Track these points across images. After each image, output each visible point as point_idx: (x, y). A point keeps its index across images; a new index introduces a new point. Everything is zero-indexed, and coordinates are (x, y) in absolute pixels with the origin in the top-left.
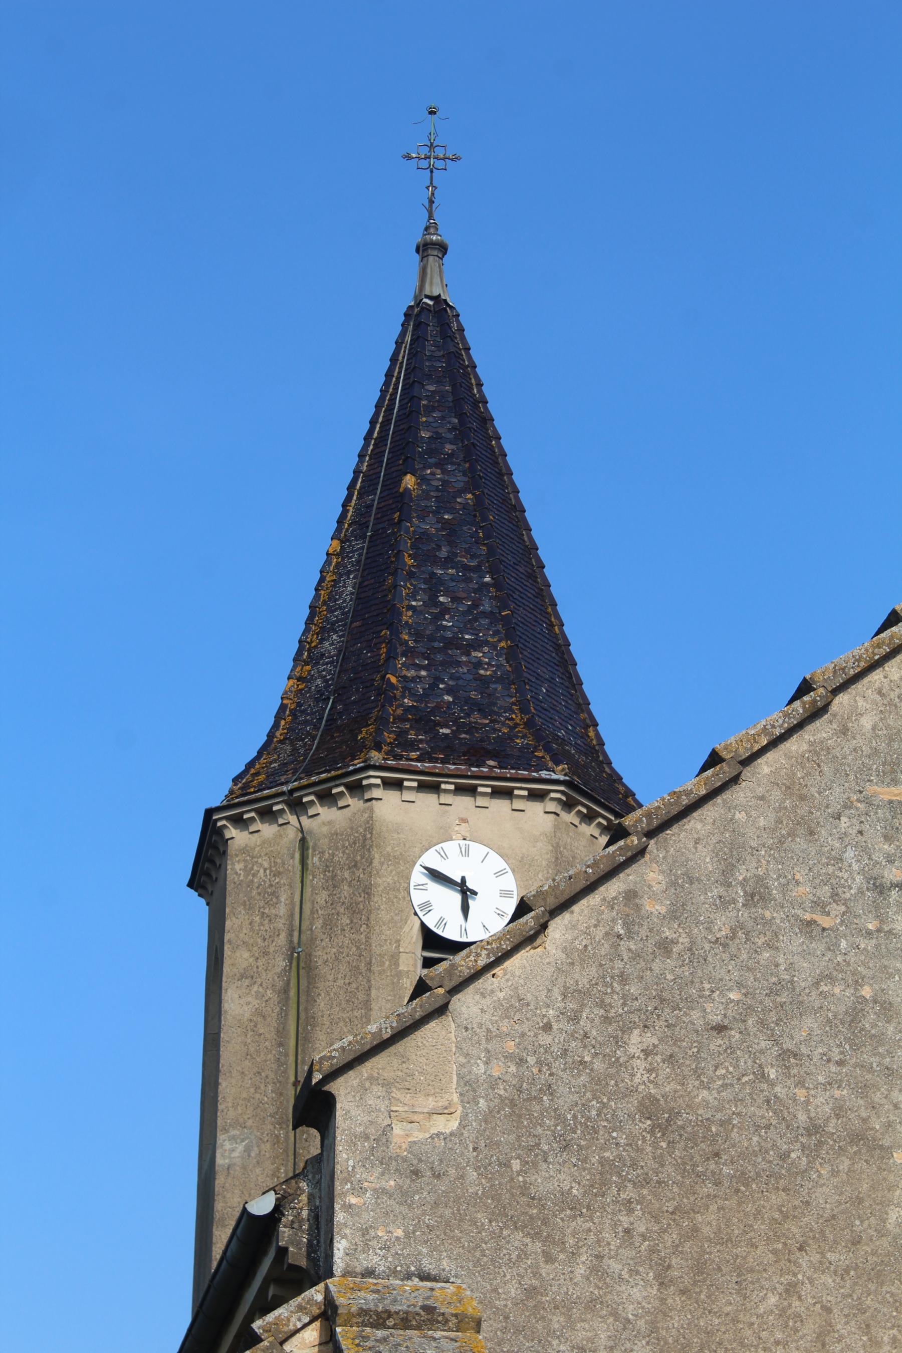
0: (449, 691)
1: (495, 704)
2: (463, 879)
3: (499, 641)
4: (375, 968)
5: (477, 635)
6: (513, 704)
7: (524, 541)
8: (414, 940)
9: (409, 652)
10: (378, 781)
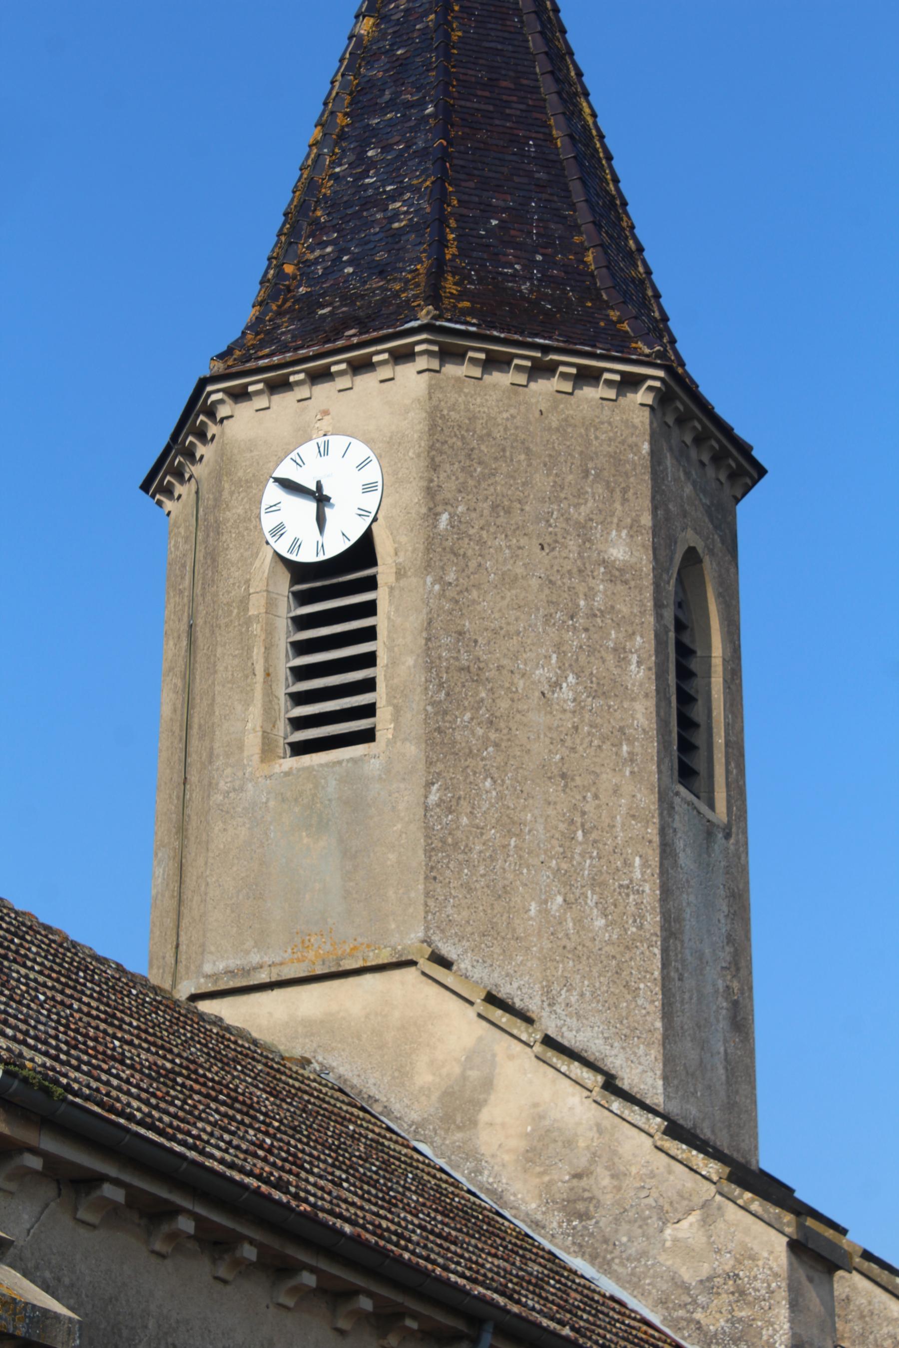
0: (349, 263)
1: (402, 260)
2: (319, 485)
3: (425, 181)
4: (223, 621)
5: (402, 182)
6: (425, 251)
7: (528, 48)
8: (266, 574)
9: (317, 228)
10: (220, 396)
